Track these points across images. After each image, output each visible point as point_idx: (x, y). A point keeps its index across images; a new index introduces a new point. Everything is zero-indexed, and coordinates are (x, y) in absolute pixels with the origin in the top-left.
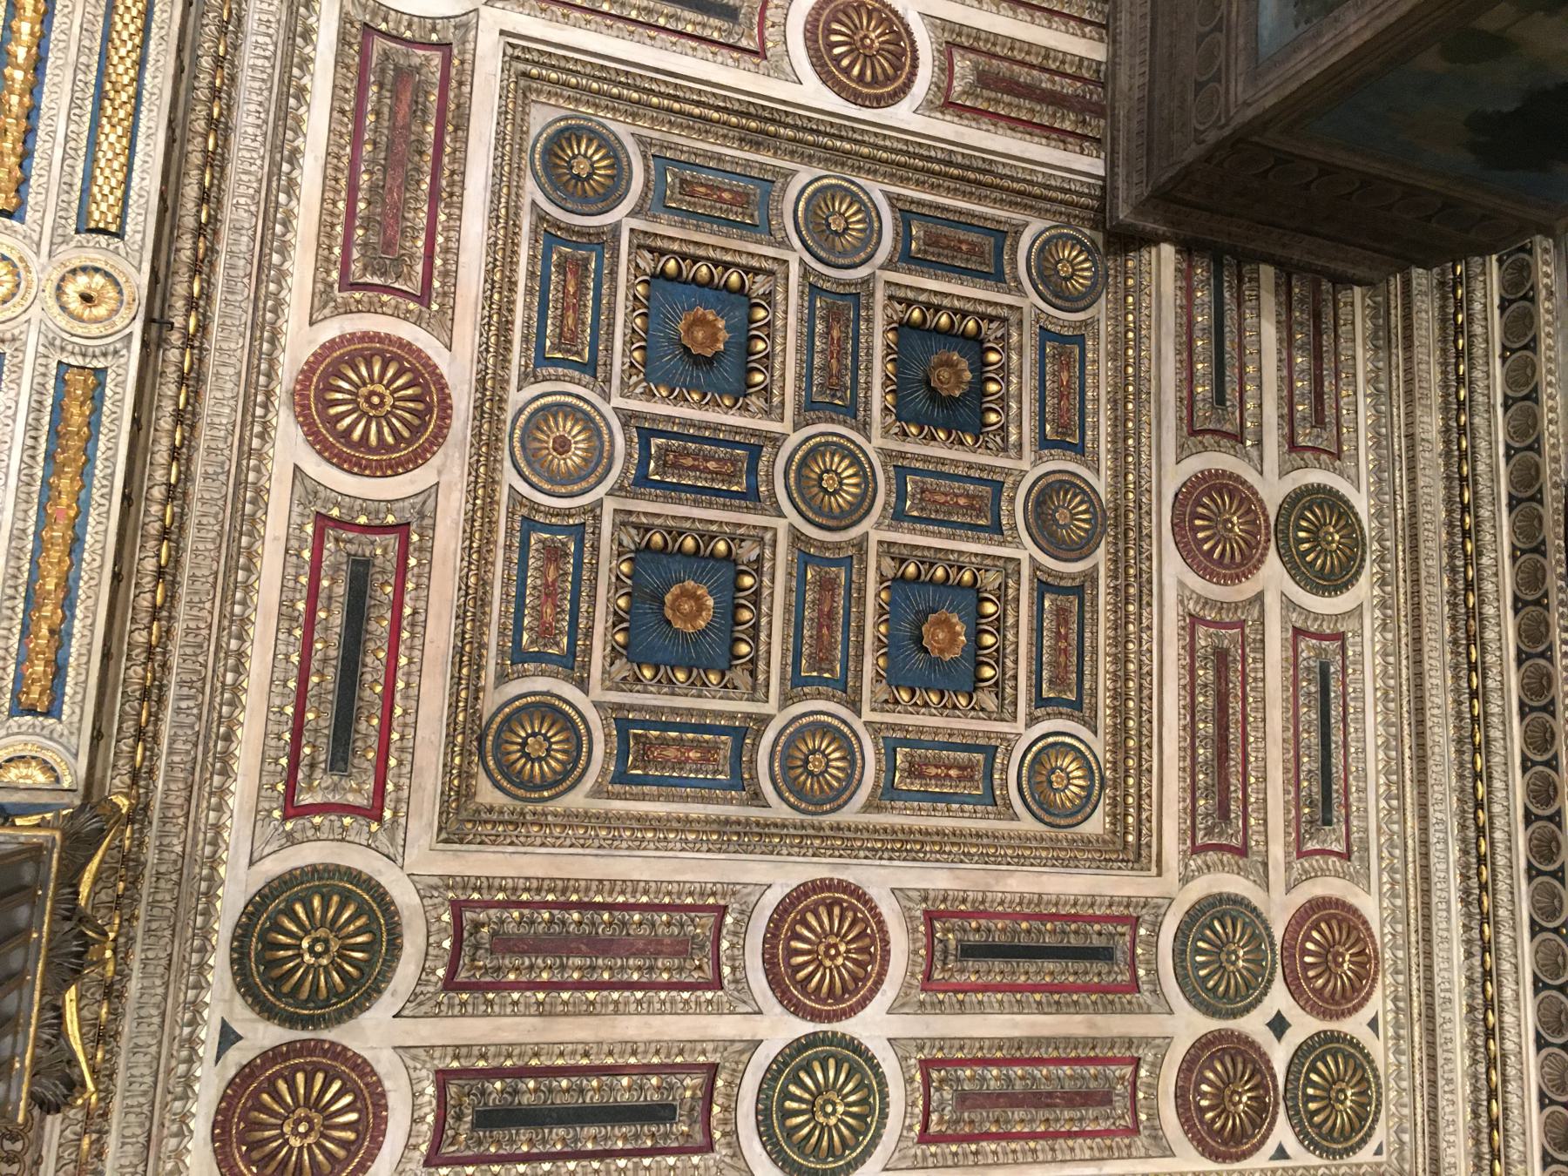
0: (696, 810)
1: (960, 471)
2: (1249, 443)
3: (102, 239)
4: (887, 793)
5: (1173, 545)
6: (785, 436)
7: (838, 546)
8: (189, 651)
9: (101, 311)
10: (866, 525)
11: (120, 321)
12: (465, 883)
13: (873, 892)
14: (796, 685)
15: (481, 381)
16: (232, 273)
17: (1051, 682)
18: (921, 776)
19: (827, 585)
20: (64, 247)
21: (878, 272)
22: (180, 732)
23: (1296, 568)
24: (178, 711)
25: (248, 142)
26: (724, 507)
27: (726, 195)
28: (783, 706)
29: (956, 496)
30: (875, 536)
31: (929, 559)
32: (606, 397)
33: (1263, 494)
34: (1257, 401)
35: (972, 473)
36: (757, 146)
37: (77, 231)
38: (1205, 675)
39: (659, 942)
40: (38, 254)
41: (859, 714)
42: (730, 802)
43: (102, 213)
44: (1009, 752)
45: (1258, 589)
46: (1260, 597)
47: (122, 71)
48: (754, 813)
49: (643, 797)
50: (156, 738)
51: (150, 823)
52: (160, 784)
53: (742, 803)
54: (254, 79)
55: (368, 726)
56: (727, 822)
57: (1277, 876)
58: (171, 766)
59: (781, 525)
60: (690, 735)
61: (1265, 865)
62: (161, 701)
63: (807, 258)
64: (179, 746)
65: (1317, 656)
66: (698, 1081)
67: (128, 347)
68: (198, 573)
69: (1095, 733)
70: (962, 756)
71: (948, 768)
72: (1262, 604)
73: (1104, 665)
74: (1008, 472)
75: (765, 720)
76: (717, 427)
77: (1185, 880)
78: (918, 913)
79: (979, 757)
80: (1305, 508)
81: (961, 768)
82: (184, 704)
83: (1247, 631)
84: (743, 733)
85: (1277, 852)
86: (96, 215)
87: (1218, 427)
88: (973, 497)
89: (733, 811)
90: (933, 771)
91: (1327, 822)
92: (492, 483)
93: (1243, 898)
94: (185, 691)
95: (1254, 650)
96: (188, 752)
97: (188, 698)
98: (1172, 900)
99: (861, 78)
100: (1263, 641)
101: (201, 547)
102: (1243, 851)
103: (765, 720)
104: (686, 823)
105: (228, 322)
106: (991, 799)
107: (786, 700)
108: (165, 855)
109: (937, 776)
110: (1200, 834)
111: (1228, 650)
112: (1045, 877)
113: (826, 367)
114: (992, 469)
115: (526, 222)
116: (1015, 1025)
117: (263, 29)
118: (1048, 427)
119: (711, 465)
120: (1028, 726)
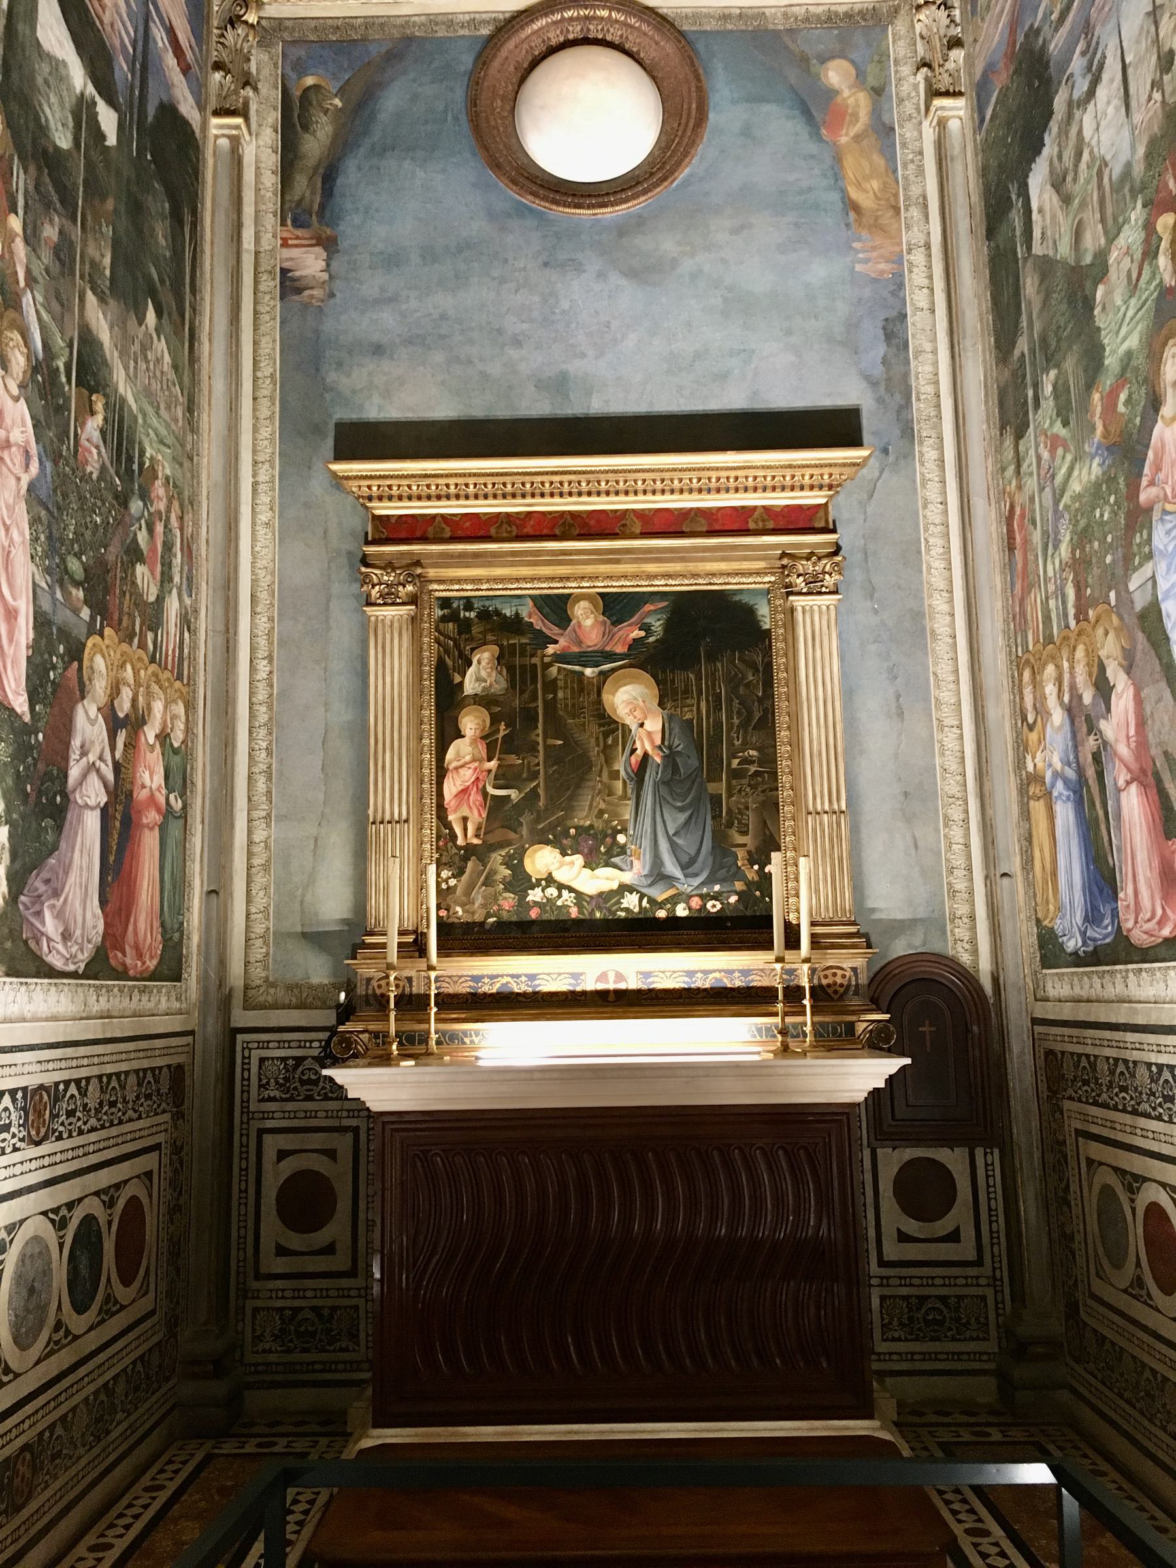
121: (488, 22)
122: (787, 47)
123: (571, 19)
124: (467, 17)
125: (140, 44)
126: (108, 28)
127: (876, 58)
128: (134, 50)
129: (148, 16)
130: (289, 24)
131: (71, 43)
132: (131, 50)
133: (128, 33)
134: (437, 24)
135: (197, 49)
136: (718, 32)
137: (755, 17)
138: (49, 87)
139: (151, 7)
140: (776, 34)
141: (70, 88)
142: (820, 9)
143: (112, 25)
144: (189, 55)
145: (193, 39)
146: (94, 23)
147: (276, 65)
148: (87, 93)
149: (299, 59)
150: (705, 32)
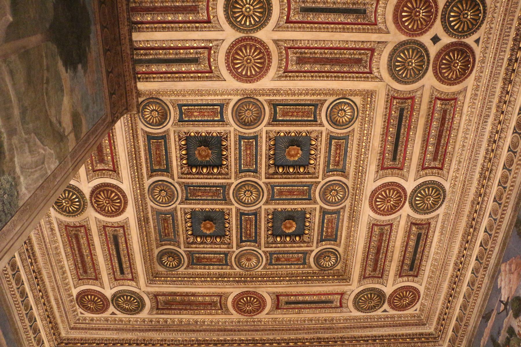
0: (345, 224)
1: (238, 152)
2: (211, 45)
4: (343, 172)
5: (259, 83)
6: (236, 207)
7: (268, 191)
10: (260, 183)
12: (360, 276)
13: (374, 188)
14: (310, 199)
15: (238, 282)
17: (309, 117)
18: (339, 162)
19: (281, 193)
21: (176, 181)
23: (261, 24)
26: (260, 222)
27: (166, 225)
28: (317, 204)
29: (247, 154)
30: (264, 180)
31: (269, 158)
32: (234, 252)
33: (233, 39)
34: (193, 42)
35: (238, 147)
36: (148, 219)
38: (307, 67)
39: (379, 240)
41: (320, 182)
42: (343, 216)
44: (332, 132)
45: (272, 42)
46: (276, 42)
48: (347, 209)
49: (341, 236)
53: (344, 212)
55: (323, 298)
56: (349, 217)
57: (383, 37)
59: (263, 207)
60: (325, 225)
61: (379, 42)
62: (320, 338)
63: (178, 202)
65: (298, 13)
66: (414, 227)
69: (326, 100)
70: (333, 148)
71: (337, 153)
72: (278, 40)
73: (302, 97)
74: (235, 135)
75: (321, 208)
76: (237, 225)
77: (381, 80)
78: (381, 172)
79: (333, 141)
80: (236, 21)
81: (337, 149)
83: (289, 46)
84: (324, 212)
85: (374, 37)
87: (207, 59)
88: (246, 148)
89: (346, 215)
90: (337, 159)
91: (364, 12)
92: (262, 276)
93: (390, 54)
95: (297, 44)
98: (387, 84)
99: (112, 192)
100: (293, 40)
102: (373, 50)
103: (321, 208)
104: (349, 228)
106: (346, 138)
107: (315, 202)
109: (339, 157)
110: (366, 70)
111: (297, 57)
112: (376, 133)
113: (212, 196)
114: (235, 141)
115: (190, 271)
116: (418, 142)
118: (216, 119)
119: (248, 226)
120: (324, 126)
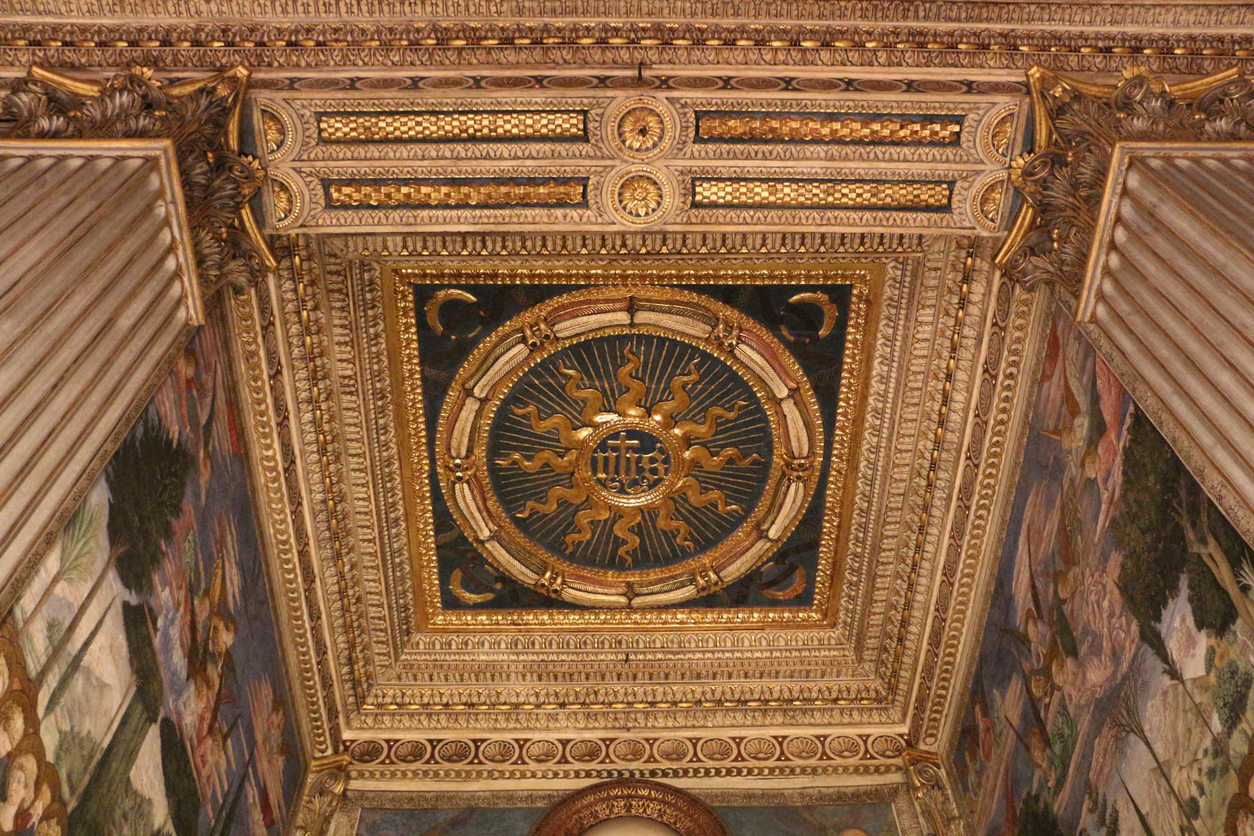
3: (591, 126)
8: (879, 14)
9: (652, 122)
11: (661, 109)
16: (559, 10)
20: (605, 150)
22: (943, 15)
24: (926, 18)
25: (439, 10)
37: (588, 141)
40: (613, 167)
43: (570, 124)
47: (451, 125)
50: (951, 34)
51: (1013, 30)
52: (983, 26)
54: (381, 11)
58: (968, 20)
64: (953, 15)
67: (678, 100)
68: (816, 13)
82: (922, 14)
86: (574, 130)
94: (911, 14)
96: (959, 8)
97: (917, 11)
101: (795, 13)
105: (602, 9)
108: (1037, 16)
117: (333, 9)
121: (544, 798)
122: (805, 820)
123: (616, 797)
124: (525, 793)
125: (232, 797)
126: (204, 780)
127: (885, 828)
128: (225, 800)
129: (244, 777)
130: (370, 795)
131: (162, 787)
132: (221, 801)
133: (222, 787)
134: (498, 798)
135: (284, 809)
136: (743, 808)
137: (774, 796)
138: (126, 820)
139: (250, 770)
140: (795, 810)
141: (149, 824)
142: (831, 790)
143: (209, 777)
144: (276, 814)
145: (282, 803)
146: (191, 773)
147: (352, 827)
148: (165, 830)
149: (375, 822)
150: (734, 808)
